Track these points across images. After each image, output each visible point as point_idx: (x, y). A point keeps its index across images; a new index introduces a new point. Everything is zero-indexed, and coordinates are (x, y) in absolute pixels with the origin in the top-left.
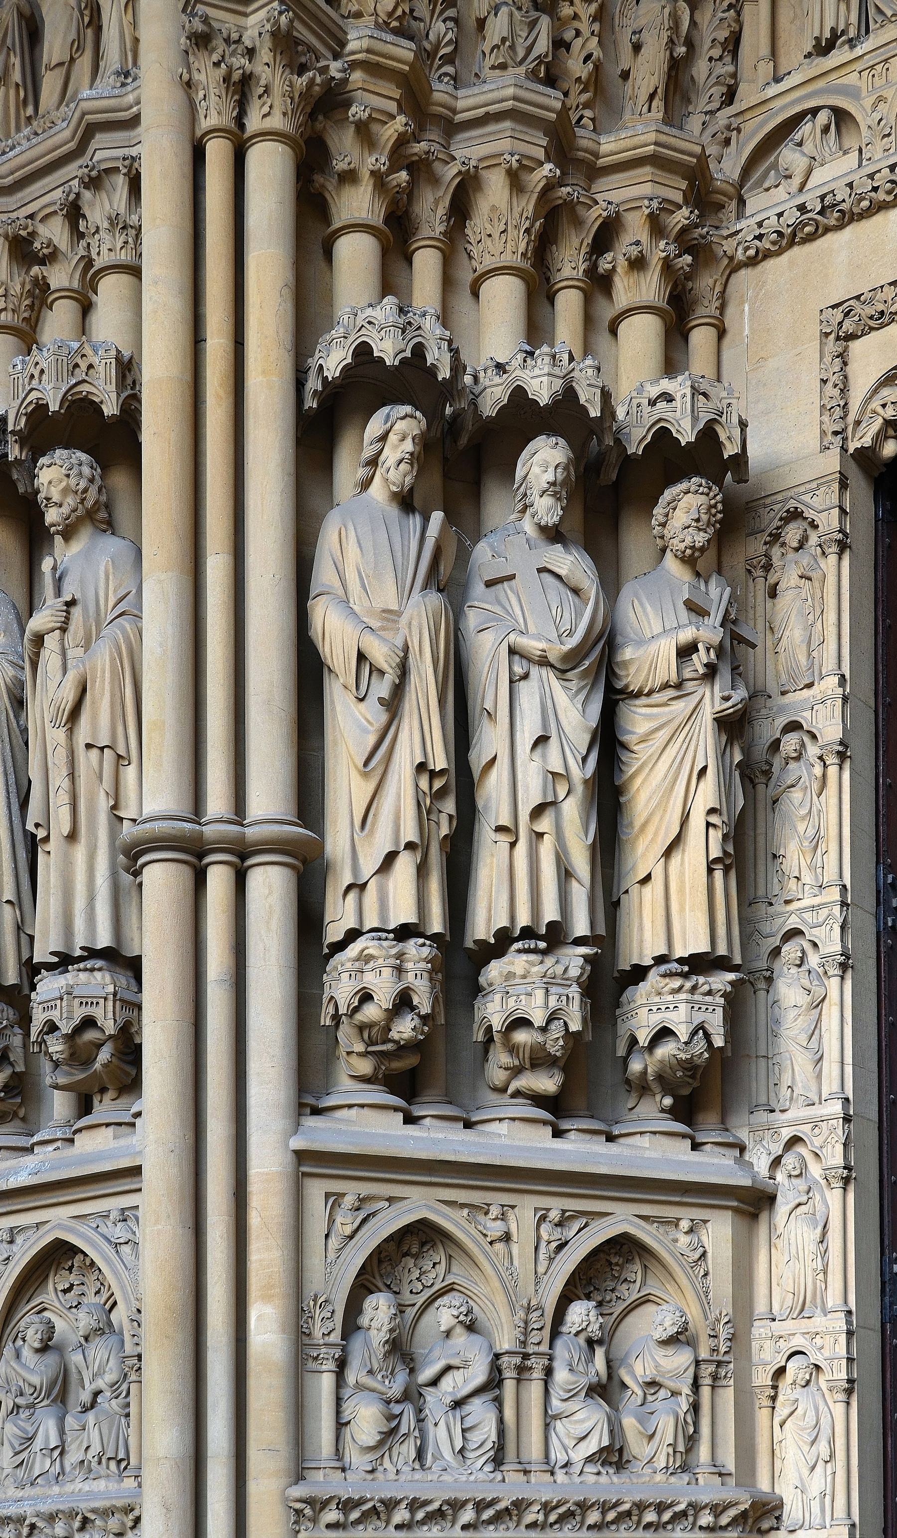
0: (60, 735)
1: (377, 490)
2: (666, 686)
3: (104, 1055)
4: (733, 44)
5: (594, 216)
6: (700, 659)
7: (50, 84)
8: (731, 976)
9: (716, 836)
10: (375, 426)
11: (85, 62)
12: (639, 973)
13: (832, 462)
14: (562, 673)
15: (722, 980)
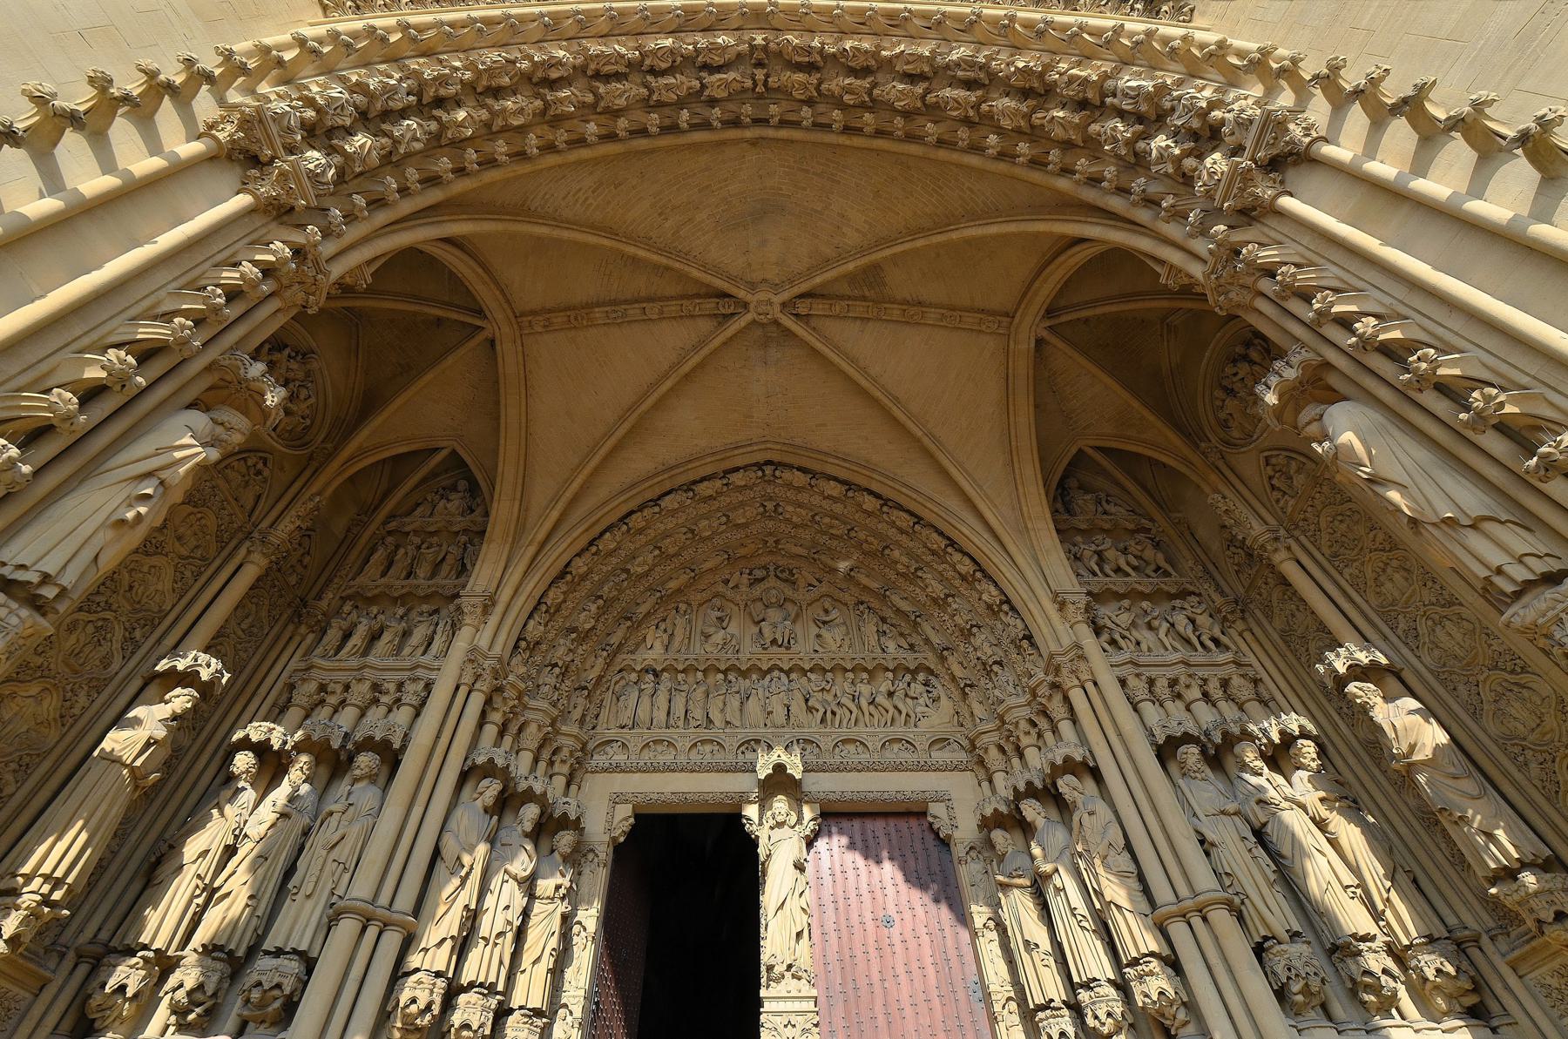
0: (325, 852)
1: (479, 803)
2: (548, 898)
3: (277, 1004)
4: (597, 716)
5: (555, 745)
6: (562, 891)
7: (407, 651)
8: (544, 1020)
9: (552, 959)
10: (485, 782)
11: (421, 649)
12: (511, 1011)
13: (606, 838)
14: (519, 883)
15: (539, 1022)
